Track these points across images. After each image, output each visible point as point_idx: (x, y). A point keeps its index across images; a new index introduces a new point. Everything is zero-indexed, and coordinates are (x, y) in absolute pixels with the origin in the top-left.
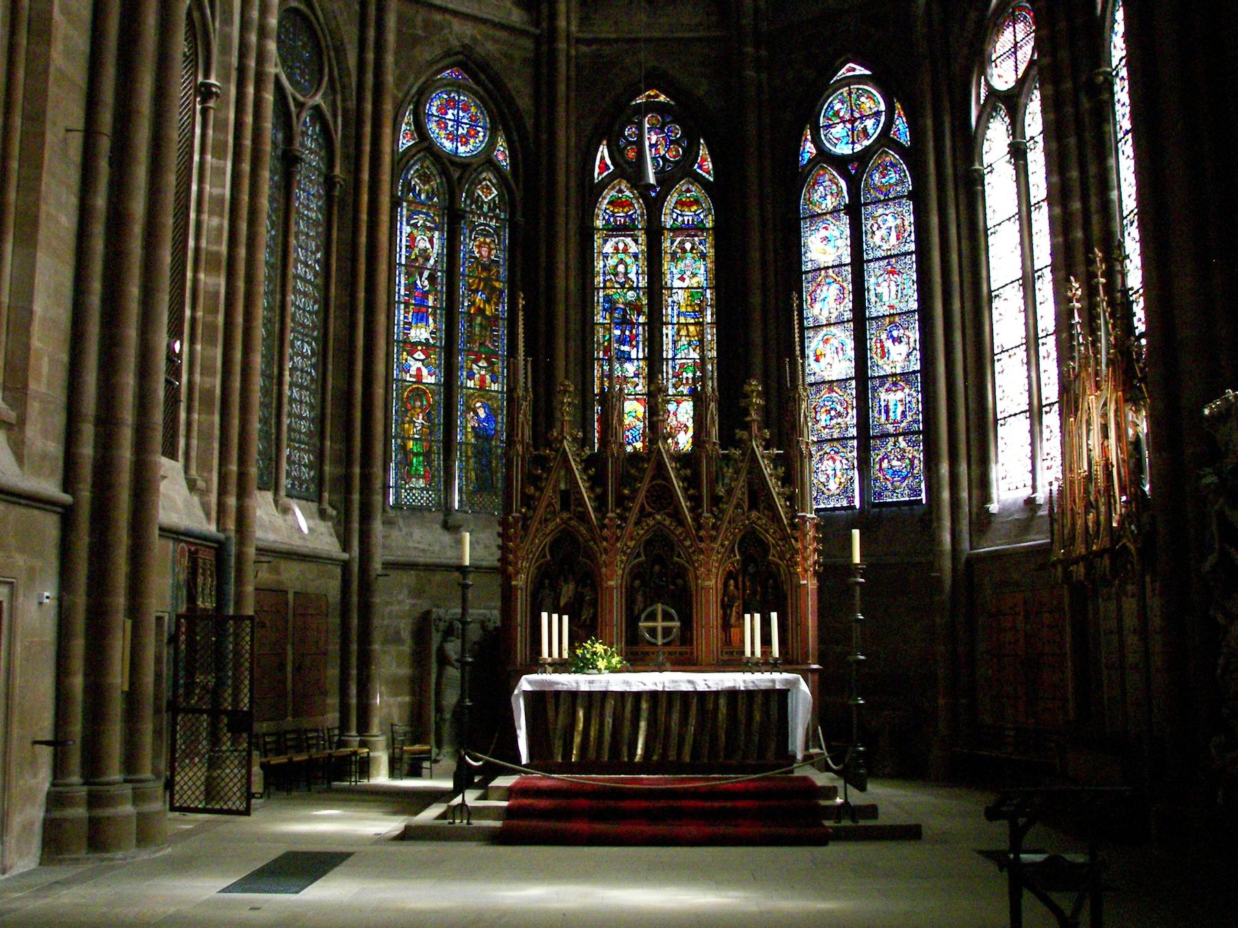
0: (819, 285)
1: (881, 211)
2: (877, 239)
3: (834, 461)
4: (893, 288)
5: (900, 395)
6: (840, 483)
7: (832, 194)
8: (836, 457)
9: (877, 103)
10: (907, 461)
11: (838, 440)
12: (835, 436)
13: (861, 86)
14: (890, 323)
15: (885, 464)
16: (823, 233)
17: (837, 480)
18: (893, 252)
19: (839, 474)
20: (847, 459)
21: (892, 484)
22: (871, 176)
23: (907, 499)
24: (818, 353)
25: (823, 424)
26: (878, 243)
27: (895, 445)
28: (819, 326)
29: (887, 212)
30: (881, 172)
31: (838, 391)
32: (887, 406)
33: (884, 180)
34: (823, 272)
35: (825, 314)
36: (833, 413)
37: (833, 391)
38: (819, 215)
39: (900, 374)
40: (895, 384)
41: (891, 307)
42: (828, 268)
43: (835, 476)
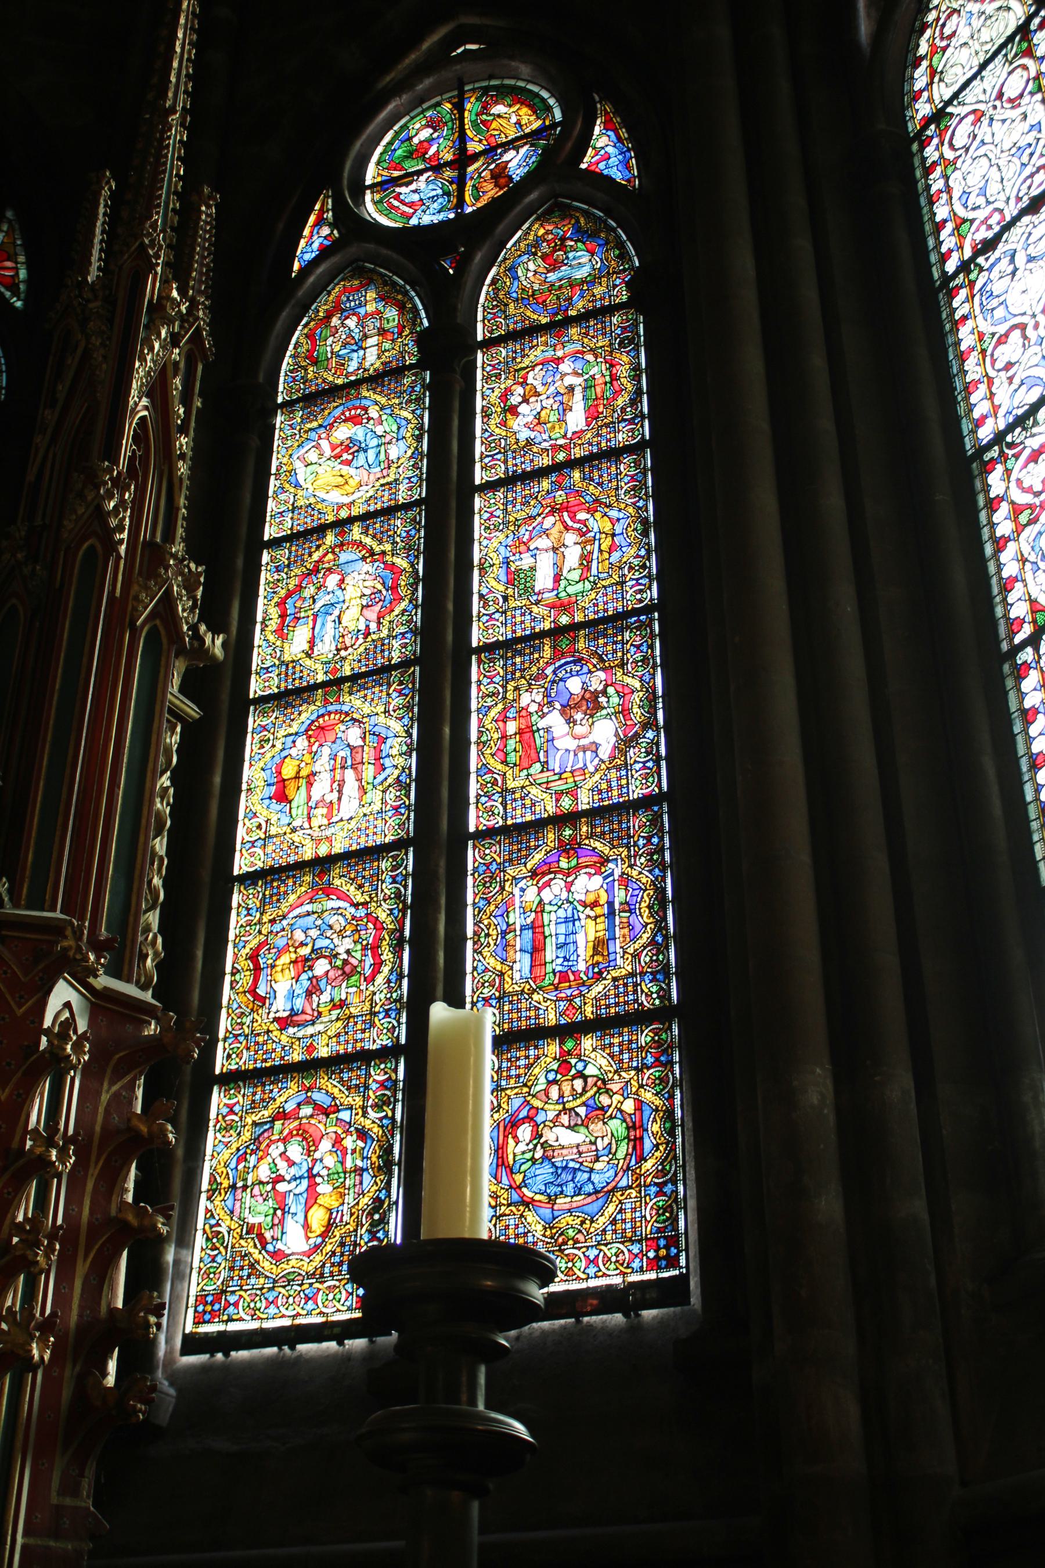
0: (316, 571)
1: (537, 354)
2: (520, 427)
3: (310, 1144)
4: (573, 556)
5: (587, 884)
6: (329, 1226)
7: (382, 332)
8: (321, 1125)
9: (539, 108)
10: (617, 1126)
11: (334, 1063)
12: (323, 1052)
13: (493, 83)
14: (557, 654)
15: (519, 1147)
16: (343, 432)
17: (318, 1218)
18: (577, 453)
19: (324, 1188)
20: (363, 1134)
21: (549, 1225)
22: (512, 269)
23: (617, 1280)
24: (288, 772)
25: (281, 1006)
26: (524, 435)
27: (564, 1066)
28: (298, 692)
29: (560, 353)
30: (544, 258)
31: (352, 890)
32: (536, 928)
33: (552, 277)
34: (330, 539)
35: (326, 648)
36: (321, 967)
37: (329, 891)
38: (333, 392)
39: (593, 813)
40: (568, 848)
41: (563, 606)
42: (351, 520)
43: (312, 1197)
